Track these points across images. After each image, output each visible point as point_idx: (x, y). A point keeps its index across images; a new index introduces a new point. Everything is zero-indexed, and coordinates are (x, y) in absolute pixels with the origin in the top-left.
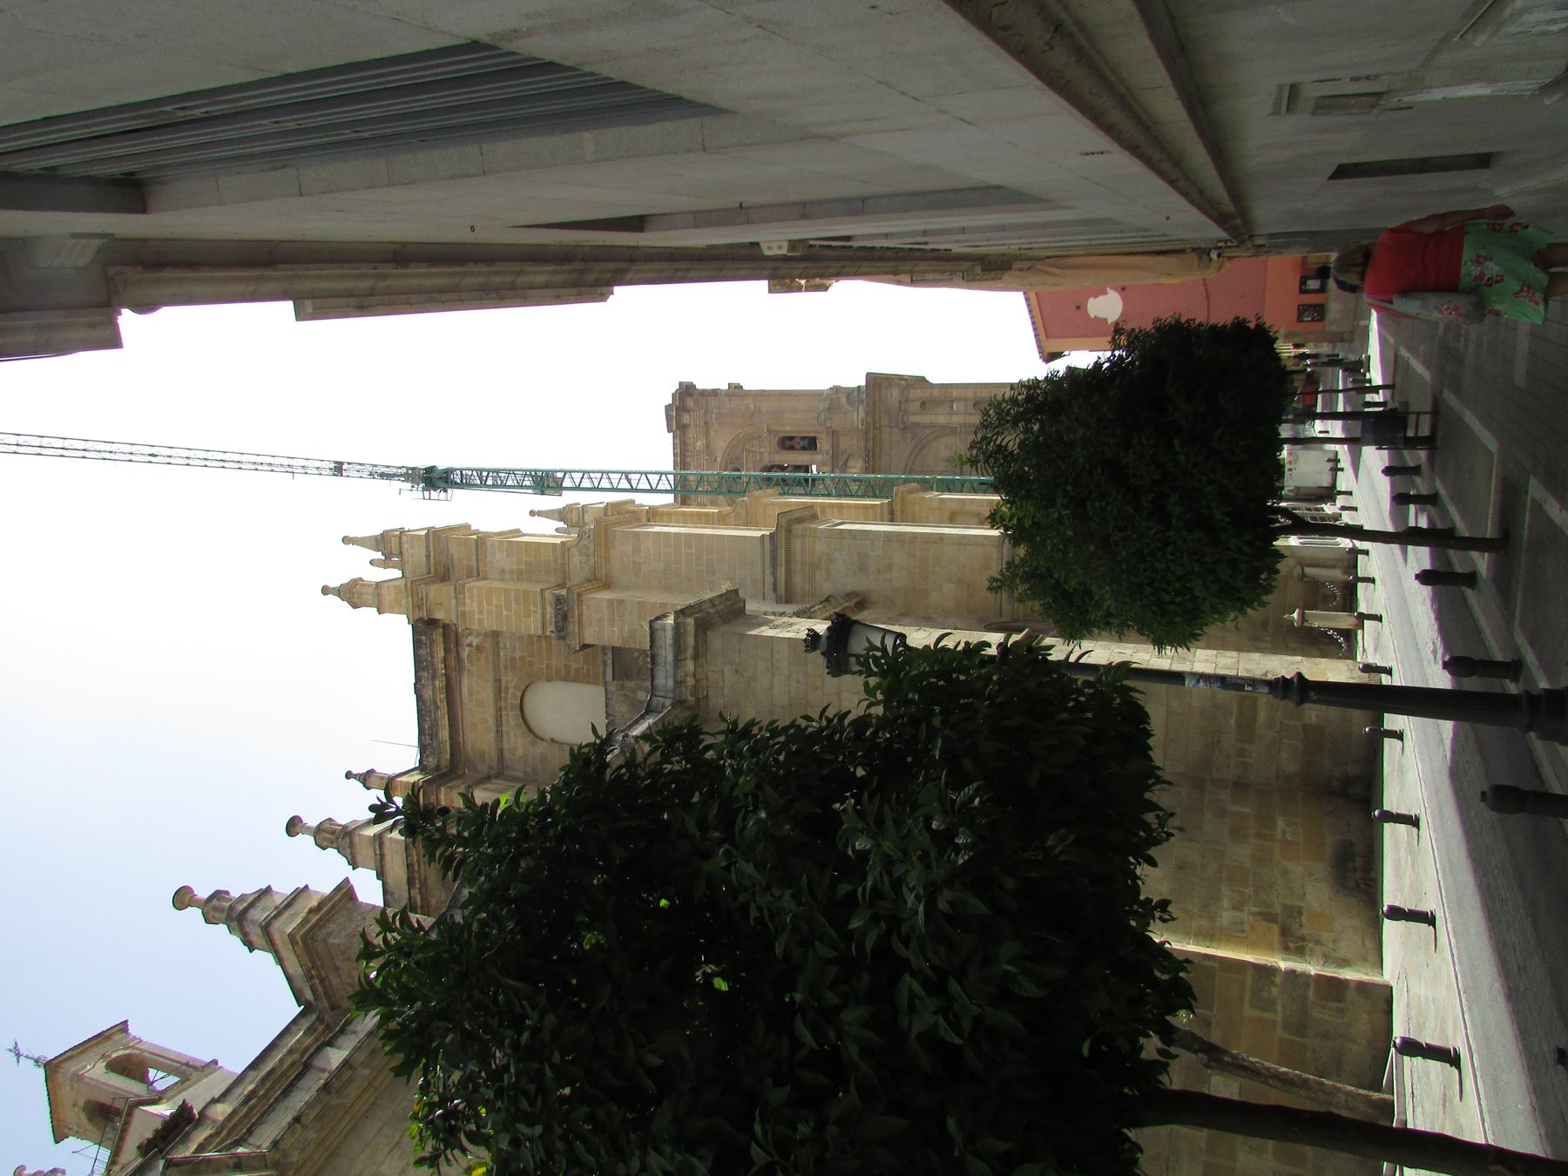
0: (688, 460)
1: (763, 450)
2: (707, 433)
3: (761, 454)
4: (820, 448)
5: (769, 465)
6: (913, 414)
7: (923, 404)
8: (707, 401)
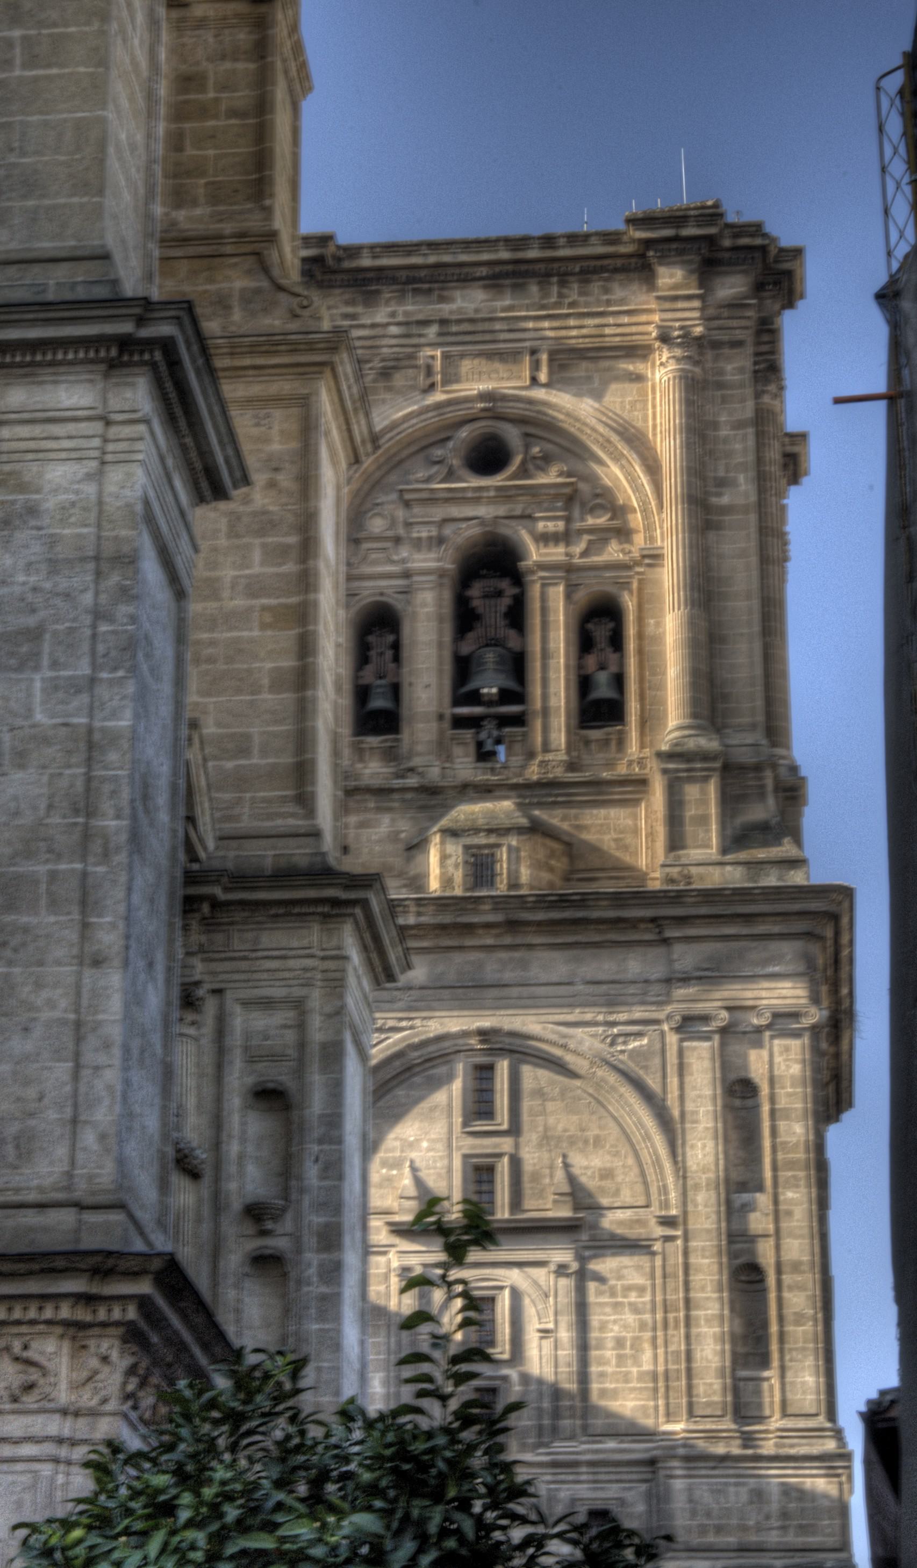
0: (534, 289)
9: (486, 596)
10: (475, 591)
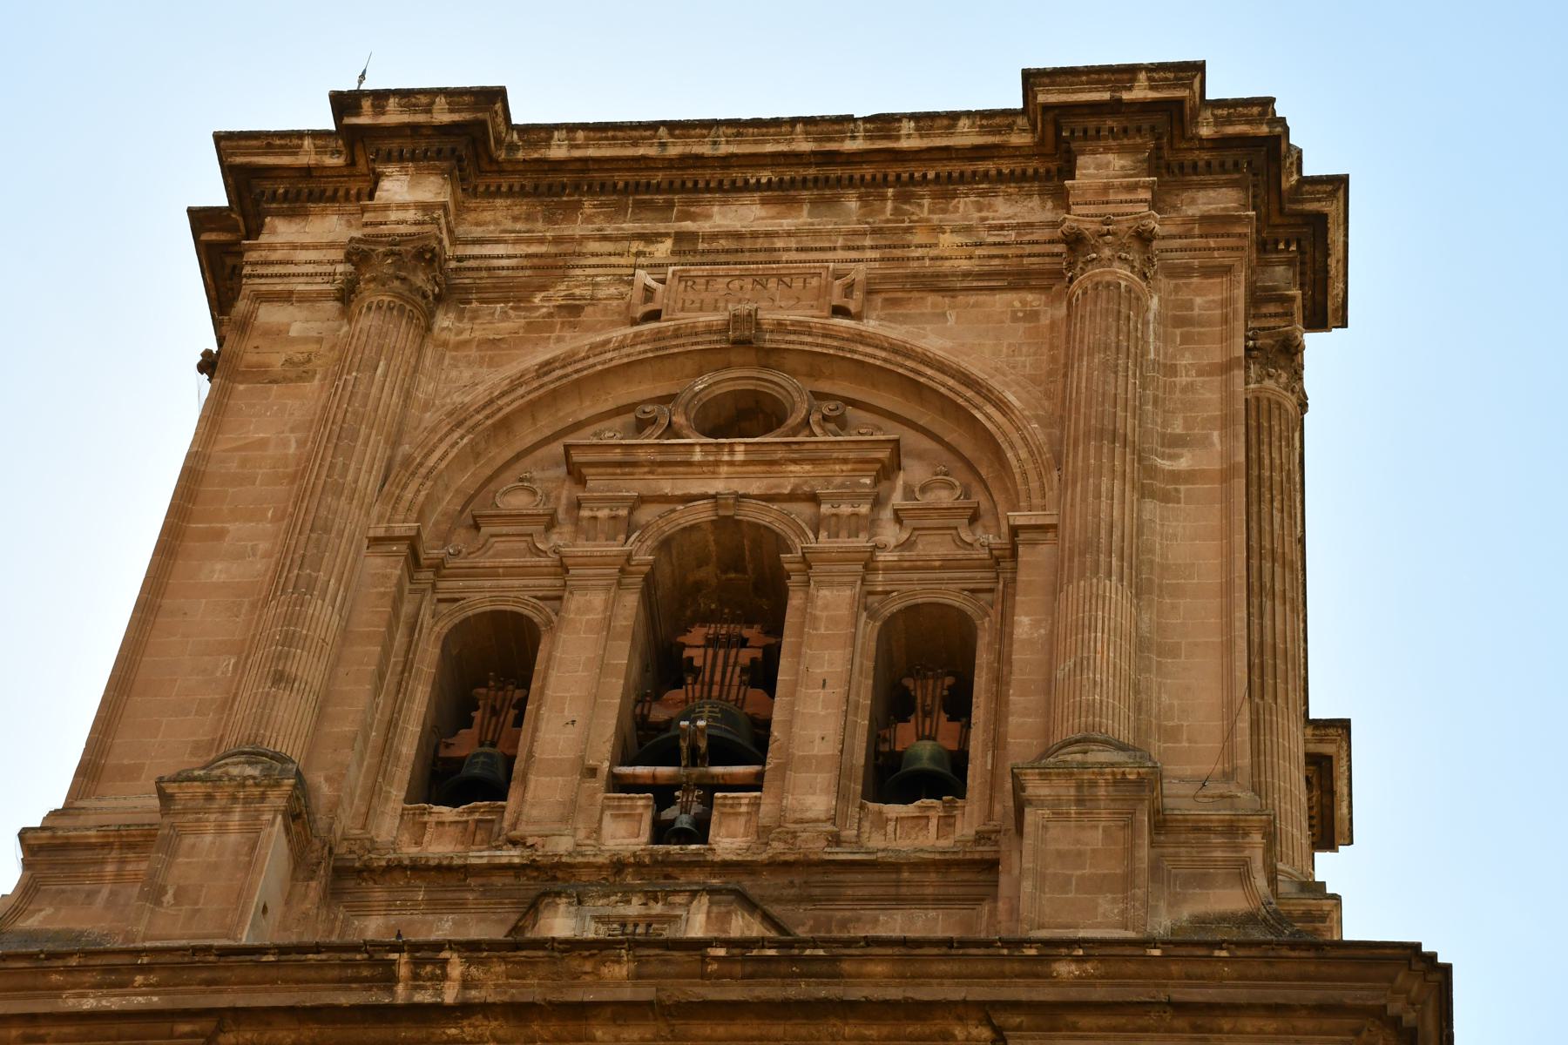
2: (1018, 280)
3: (872, 524)
4: (881, 822)
8: (1208, 272)
9: (712, 642)
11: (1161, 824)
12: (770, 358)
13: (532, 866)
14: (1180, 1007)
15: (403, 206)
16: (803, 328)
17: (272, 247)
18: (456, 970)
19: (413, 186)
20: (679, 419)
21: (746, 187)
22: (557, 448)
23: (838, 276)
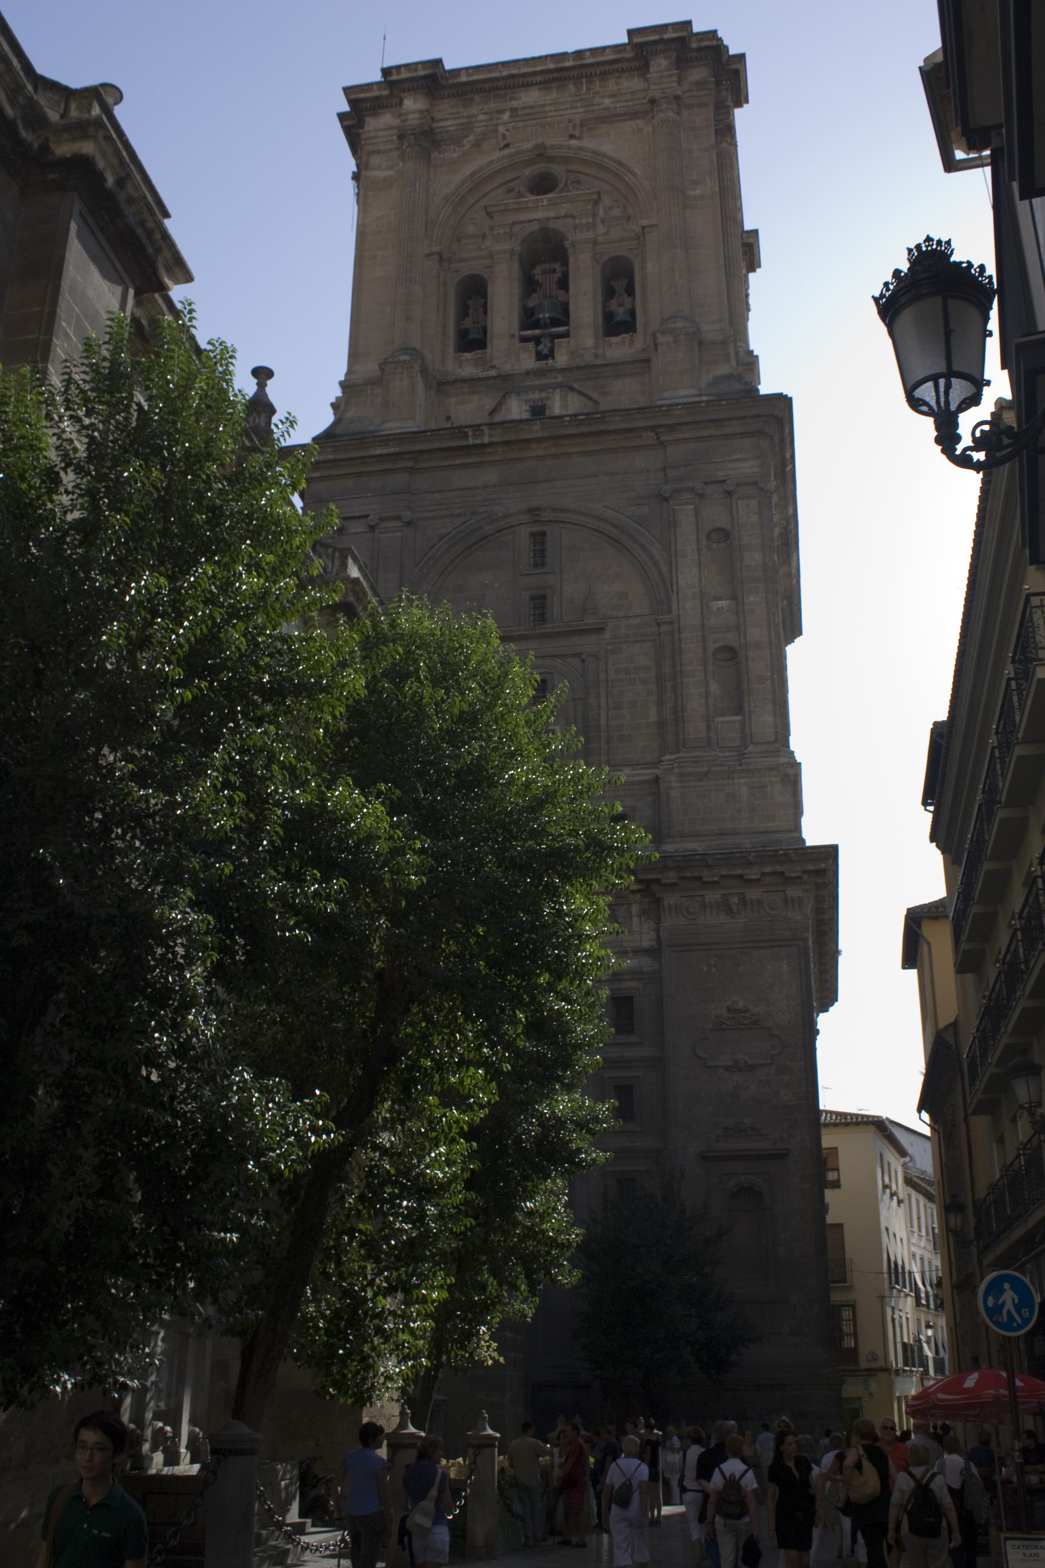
0: (571, 87)
1: (601, 229)
2: (634, 115)
5: (567, 244)
6: (697, 512)
7: (724, 534)
10: (538, 270)
11: (701, 343)
12: (550, 159)
13: (499, 376)
14: (711, 421)
15: (414, 112)
16: (561, 147)
17: (369, 131)
18: (486, 431)
19: (415, 102)
20: (522, 189)
21: (533, 84)
22: (482, 203)
23: (570, 121)
